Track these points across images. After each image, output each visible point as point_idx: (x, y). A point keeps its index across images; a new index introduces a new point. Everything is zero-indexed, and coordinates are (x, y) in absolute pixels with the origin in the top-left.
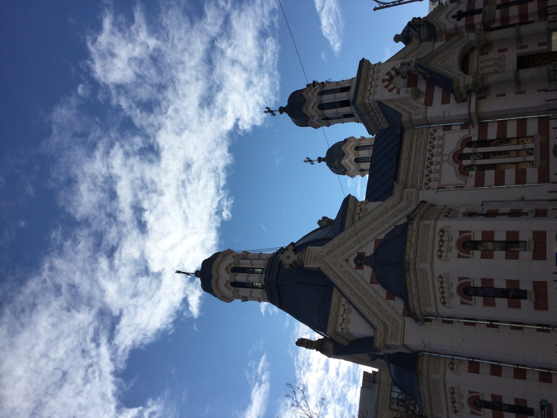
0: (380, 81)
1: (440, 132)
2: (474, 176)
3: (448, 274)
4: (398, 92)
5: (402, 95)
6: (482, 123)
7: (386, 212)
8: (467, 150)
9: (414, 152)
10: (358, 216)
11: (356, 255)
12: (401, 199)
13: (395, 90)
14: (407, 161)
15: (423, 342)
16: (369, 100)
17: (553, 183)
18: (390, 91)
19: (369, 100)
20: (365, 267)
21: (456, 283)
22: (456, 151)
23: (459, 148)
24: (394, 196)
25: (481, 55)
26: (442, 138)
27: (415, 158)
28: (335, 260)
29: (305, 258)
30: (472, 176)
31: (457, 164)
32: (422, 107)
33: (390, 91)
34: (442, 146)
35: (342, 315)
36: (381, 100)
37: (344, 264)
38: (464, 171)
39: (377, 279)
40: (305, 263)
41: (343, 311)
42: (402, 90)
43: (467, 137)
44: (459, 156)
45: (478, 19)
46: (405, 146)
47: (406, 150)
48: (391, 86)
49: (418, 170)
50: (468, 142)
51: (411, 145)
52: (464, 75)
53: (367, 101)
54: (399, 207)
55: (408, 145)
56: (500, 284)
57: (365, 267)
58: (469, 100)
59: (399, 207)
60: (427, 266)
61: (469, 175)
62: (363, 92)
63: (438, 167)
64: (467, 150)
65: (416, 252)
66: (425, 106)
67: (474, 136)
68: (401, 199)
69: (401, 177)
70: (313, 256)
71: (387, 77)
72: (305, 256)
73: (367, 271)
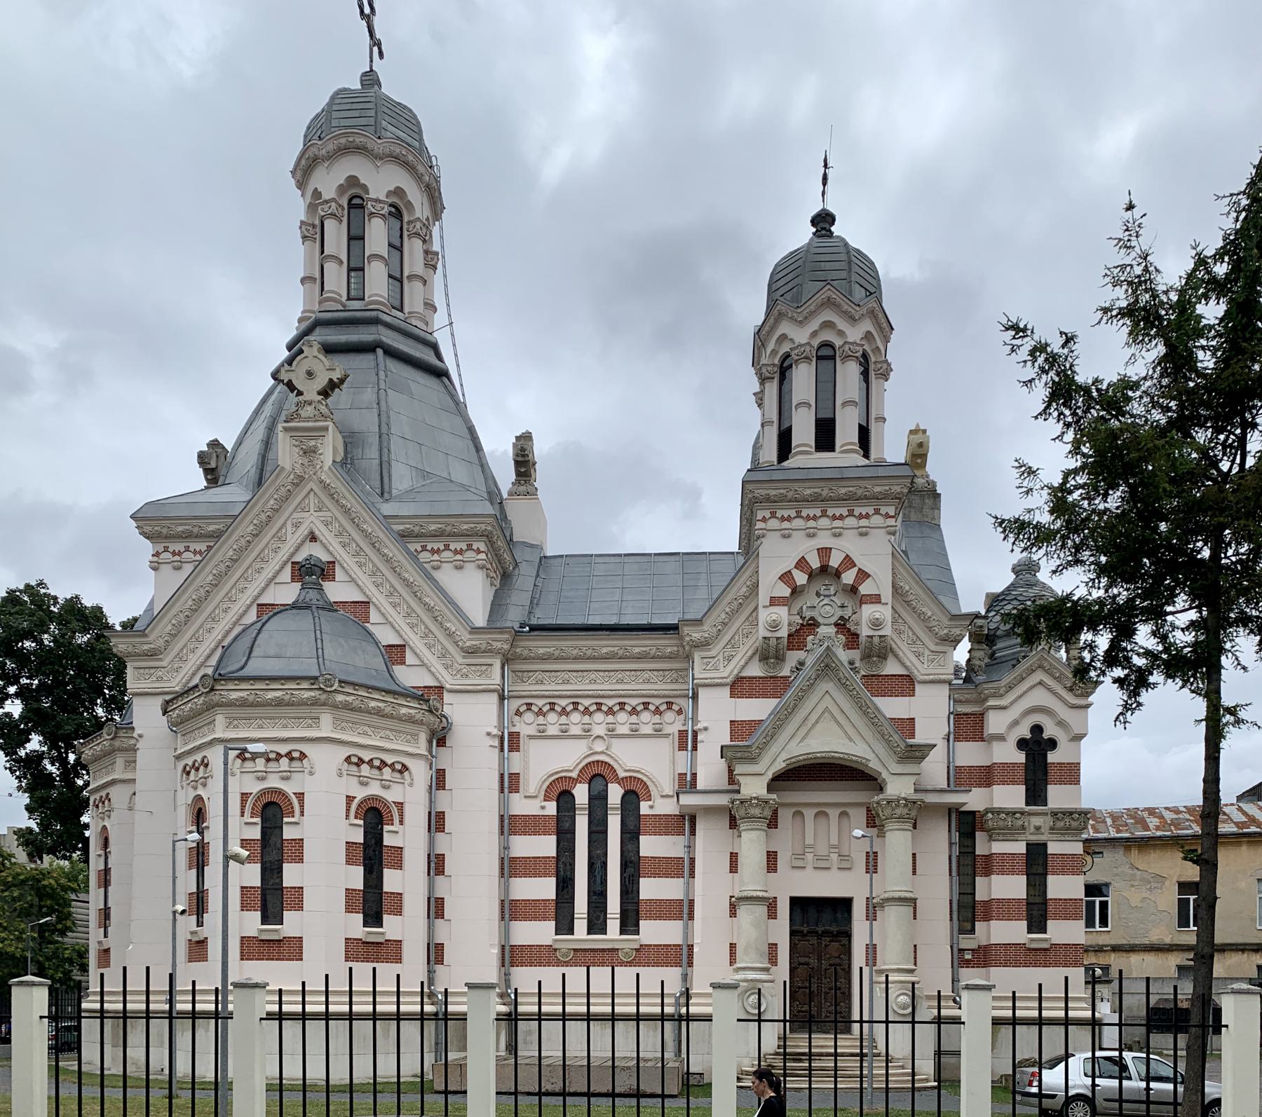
1: (673, 724)
3: (311, 773)
4: (774, 601)
5: (766, 615)
8: (615, 794)
10: (442, 548)
11: (325, 558)
14: (589, 653)
15: (140, 736)
20: (298, 585)
21: (289, 788)
22: (616, 766)
23: (622, 774)
30: (543, 808)
31: (577, 773)
32: (728, 672)
42: (781, 613)
43: (651, 787)
44: (598, 775)
52: (770, 775)
56: (356, 877)
57: (298, 585)
61: (545, 800)
64: (615, 794)
67: (651, 807)
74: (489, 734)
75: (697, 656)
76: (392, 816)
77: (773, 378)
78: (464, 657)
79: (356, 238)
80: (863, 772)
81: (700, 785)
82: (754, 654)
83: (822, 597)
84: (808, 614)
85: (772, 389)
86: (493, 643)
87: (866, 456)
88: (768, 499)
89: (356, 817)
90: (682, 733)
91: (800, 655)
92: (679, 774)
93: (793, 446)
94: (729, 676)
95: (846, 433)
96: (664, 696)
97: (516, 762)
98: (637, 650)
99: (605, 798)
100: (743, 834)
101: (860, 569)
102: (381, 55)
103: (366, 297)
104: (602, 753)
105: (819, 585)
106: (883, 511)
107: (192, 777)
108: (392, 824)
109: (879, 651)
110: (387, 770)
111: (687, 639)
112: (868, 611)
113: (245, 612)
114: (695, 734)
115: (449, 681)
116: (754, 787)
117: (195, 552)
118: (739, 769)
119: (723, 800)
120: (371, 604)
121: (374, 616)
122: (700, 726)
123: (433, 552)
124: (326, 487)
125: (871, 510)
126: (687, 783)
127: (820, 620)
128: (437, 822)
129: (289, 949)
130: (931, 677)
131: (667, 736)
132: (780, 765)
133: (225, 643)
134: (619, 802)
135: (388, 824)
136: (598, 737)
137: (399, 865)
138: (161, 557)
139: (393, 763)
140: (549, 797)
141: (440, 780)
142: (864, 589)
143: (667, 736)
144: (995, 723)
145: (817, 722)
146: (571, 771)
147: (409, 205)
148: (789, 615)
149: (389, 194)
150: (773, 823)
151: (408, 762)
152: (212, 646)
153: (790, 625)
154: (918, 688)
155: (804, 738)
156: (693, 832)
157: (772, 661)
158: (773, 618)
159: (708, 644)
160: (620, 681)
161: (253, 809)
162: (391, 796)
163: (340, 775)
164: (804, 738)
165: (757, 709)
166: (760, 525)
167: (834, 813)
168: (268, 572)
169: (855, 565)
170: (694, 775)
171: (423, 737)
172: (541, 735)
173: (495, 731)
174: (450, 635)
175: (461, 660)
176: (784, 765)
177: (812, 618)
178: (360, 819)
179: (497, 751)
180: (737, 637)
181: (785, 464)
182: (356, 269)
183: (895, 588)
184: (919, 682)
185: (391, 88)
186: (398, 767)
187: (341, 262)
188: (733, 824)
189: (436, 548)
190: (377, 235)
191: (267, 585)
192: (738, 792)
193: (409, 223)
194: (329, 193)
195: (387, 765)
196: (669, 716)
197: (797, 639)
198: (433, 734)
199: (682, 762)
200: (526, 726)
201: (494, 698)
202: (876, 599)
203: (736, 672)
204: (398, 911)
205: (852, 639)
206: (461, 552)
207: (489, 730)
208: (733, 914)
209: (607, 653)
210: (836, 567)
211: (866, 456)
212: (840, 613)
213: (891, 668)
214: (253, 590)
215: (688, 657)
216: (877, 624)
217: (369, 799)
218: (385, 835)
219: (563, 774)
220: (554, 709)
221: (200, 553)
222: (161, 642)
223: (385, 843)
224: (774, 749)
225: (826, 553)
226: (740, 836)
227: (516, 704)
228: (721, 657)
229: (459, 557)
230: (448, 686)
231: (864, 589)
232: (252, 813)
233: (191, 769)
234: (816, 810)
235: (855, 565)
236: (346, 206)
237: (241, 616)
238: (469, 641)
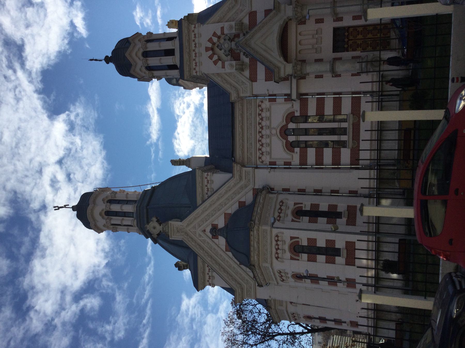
0: (203, 50)
2: (299, 153)
4: (223, 67)
6: (302, 98)
7: (230, 190)
8: (292, 126)
9: (246, 125)
12: (241, 178)
13: (220, 63)
14: (241, 136)
16: (196, 72)
17: (358, 267)
18: (215, 63)
19: (196, 72)
20: (220, 237)
23: (285, 123)
24: (234, 178)
25: (299, 24)
26: (269, 110)
27: (247, 140)
28: (194, 230)
29: (169, 231)
30: (297, 153)
32: (248, 83)
33: (215, 63)
34: (269, 118)
35: (208, 274)
36: (208, 74)
37: (202, 234)
38: (290, 146)
39: (230, 246)
40: (170, 235)
41: (208, 270)
42: (227, 64)
44: (284, 132)
46: (237, 119)
47: (239, 124)
48: (215, 57)
49: (251, 143)
50: (291, 118)
51: (242, 117)
52: (285, 63)
53: (195, 74)
54: (239, 185)
55: (240, 118)
58: (290, 79)
59: (239, 185)
60: (268, 265)
61: (294, 152)
62: (188, 63)
63: (268, 141)
65: (258, 255)
66: (251, 83)
68: (241, 178)
69: (238, 151)
70: (175, 228)
71: (210, 45)
72: (169, 229)
73: (222, 241)
75: (242, 95)
77: (153, 73)
79: (116, 214)
80: (284, 28)
81: (288, 92)
82: (241, 74)
83: (222, 48)
84: (227, 53)
85: (156, 73)
86: (238, 170)
87: (176, 38)
88: (190, 71)
89: (299, 219)
90: (270, 100)
91: (242, 54)
92: (285, 101)
93: (173, 64)
95: (167, 45)
97: (280, 163)
99: (293, 129)
100: (308, 72)
101: (213, 36)
102: (68, 205)
103: (132, 211)
105: (217, 50)
106: (193, 29)
107: (284, 278)
109: (240, 24)
110: (282, 208)
111: (236, 99)
112: (226, 32)
113: (228, 256)
114: (270, 95)
115: (251, 186)
116: (288, 69)
117: (209, 271)
118: (282, 75)
119: (294, 81)
120: (226, 212)
121: (229, 211)
122: (267, 93)
124: (188, 225)
125: (193, 34)
126: (288, 98)
127: (229, 48)
128: (302, 192)
129: (351, 247)
131: (270, 107)
132: (282, 59)
133: (238, 263)
134: (295, 124)
136: (271, 133)
137: (318, 205)
138: (211, 283)
139: (280, 205)
140: (293, 150)
141: (286, 190)
142: (219, 33)
143: (270, 107)
145: (265, 46)
146: (283, 142)
147: (107, 197)
148: (228, 61)
149: (104, 203)
150: (304, 61)
151: (278, 202)
152: (240, 268)
153: (231, 60)
156: (307, 94)
157: (244, 67)
158: (229, 66)
161: (296, 256)
162: (292, 207)
165: (261, 70)
166: (198, 74)
167: (299, 38)
169: (211, 38)
170: (286, 95)
171: (271, 195)
173: (269, 170)
174: (235, 185)
176: (282, 58)
177: (229, 51)
178: (300, 217)
179: (275, 169)
180: (236, 80)
181: (178, 66)
182: (125, 214)
183: (218, 22)
184: (251, 10)
185: (75, 203)
186: (281, 204)
187: (123, 219)
188: (304, 78)
189: (207, 190)
190: (115, 208)
192: (291, 75)
193: (112, 197)
194: (104, 222)
195: (280, 208)
196: (263, 106)
197: (234, 55)
198: (269, 192)
199: (280, 100)
200: (267, 159)
201: (256, 170)
202: (222, 28)
203: (248, 80)
204: (336, 206)
205: (237, 36)
206: (208, 181)
208: (340, 76)
209: (241, 129)
210: (211, 44)
211: (176, 38)
212: (227, 41)
213: (246, 21)
214: (220, 252)
215: (242, 99)
216: (231, 27)
217: (293, 214)
218: (306, 209)
219: (284, 145)
220: (261, 149)
221: (209, 269)
223: (309, 209)
225: (207, 49)
226: (309, 73)
227: (259, 162)
228: (242, 86)
230: (253, 187)
231: (219, 33)
232: (298, 256)
233: (282, 278)
234: (298, 35)
235: (211, 38)
236: (107, 217)
237: (230, 257)
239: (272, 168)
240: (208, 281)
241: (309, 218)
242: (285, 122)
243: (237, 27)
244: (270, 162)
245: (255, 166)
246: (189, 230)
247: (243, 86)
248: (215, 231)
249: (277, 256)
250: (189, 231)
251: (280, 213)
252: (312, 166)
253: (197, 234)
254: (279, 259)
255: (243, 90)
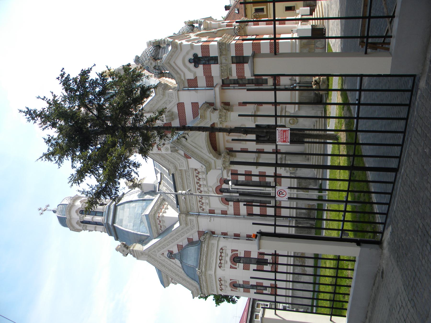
23: (219, 184)
32: (183, 160)
34: (206, 179)
37: (161, 256)
38: (226, 201)
45: (215, 69)
51: (182, 179)
52: (214, 159)
61: (229, 205)
66: (185, 159)
70: (139, 253)
74: (210, 221)
76: (235, 254)
78: (189, 226)
94: (185, 160)
96: (193, 172)
97: (218, 211)
98: (180, 180)
104: (213, 189)
108: (238, 254)
115: (196, 230)
123: (161, 227)
130: (177, 98)
135: (238, 255)
136: (208, 190)
137: (249, 252)
144: (190, 76)
145: (196, 144)
154: (181, 101)
155: (202, 148)
159: (176, 166)
160: (190, 183)
163: (224, 270)
164: (202, 148)
168: (172, 264)
172: (209, 204)
175: (190, 226)
176: (211, 154)
191: (176, 265)
200: (207, 208)
203: (183, 158)
207: (209, 221)
219: (221, 200)
222: (194, 288)
224: (206, 157)
228: (179, 162)
229: (161, 221)
238: (184, 225)
239: (211, 216)
240: (171, 281)
241: (244, 264)
242: (219, 183)
243: (167, 118)
244: (209, 210)
245: (198, 214)
246: (151, 253)
247: (179, 161)
248: (171, 255)
249: (221, 258)
250: (151, 254)
251: (220, 260)
252: (244, 216)
253: (158, 256)
254: (222, 291)
255: (180, 165)
